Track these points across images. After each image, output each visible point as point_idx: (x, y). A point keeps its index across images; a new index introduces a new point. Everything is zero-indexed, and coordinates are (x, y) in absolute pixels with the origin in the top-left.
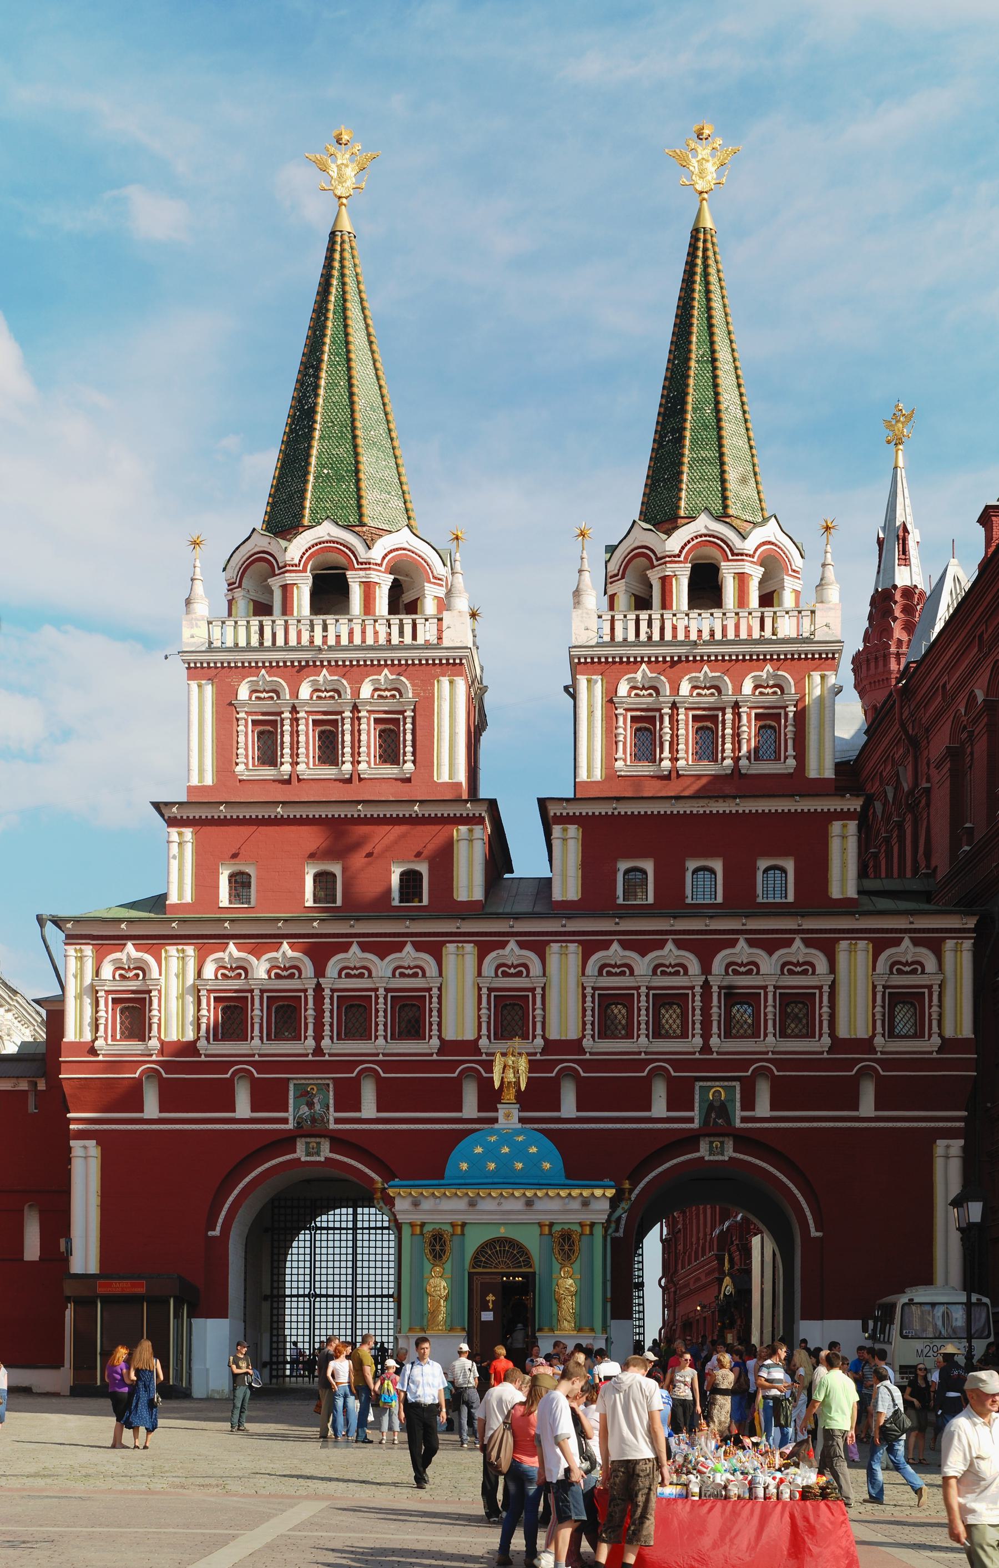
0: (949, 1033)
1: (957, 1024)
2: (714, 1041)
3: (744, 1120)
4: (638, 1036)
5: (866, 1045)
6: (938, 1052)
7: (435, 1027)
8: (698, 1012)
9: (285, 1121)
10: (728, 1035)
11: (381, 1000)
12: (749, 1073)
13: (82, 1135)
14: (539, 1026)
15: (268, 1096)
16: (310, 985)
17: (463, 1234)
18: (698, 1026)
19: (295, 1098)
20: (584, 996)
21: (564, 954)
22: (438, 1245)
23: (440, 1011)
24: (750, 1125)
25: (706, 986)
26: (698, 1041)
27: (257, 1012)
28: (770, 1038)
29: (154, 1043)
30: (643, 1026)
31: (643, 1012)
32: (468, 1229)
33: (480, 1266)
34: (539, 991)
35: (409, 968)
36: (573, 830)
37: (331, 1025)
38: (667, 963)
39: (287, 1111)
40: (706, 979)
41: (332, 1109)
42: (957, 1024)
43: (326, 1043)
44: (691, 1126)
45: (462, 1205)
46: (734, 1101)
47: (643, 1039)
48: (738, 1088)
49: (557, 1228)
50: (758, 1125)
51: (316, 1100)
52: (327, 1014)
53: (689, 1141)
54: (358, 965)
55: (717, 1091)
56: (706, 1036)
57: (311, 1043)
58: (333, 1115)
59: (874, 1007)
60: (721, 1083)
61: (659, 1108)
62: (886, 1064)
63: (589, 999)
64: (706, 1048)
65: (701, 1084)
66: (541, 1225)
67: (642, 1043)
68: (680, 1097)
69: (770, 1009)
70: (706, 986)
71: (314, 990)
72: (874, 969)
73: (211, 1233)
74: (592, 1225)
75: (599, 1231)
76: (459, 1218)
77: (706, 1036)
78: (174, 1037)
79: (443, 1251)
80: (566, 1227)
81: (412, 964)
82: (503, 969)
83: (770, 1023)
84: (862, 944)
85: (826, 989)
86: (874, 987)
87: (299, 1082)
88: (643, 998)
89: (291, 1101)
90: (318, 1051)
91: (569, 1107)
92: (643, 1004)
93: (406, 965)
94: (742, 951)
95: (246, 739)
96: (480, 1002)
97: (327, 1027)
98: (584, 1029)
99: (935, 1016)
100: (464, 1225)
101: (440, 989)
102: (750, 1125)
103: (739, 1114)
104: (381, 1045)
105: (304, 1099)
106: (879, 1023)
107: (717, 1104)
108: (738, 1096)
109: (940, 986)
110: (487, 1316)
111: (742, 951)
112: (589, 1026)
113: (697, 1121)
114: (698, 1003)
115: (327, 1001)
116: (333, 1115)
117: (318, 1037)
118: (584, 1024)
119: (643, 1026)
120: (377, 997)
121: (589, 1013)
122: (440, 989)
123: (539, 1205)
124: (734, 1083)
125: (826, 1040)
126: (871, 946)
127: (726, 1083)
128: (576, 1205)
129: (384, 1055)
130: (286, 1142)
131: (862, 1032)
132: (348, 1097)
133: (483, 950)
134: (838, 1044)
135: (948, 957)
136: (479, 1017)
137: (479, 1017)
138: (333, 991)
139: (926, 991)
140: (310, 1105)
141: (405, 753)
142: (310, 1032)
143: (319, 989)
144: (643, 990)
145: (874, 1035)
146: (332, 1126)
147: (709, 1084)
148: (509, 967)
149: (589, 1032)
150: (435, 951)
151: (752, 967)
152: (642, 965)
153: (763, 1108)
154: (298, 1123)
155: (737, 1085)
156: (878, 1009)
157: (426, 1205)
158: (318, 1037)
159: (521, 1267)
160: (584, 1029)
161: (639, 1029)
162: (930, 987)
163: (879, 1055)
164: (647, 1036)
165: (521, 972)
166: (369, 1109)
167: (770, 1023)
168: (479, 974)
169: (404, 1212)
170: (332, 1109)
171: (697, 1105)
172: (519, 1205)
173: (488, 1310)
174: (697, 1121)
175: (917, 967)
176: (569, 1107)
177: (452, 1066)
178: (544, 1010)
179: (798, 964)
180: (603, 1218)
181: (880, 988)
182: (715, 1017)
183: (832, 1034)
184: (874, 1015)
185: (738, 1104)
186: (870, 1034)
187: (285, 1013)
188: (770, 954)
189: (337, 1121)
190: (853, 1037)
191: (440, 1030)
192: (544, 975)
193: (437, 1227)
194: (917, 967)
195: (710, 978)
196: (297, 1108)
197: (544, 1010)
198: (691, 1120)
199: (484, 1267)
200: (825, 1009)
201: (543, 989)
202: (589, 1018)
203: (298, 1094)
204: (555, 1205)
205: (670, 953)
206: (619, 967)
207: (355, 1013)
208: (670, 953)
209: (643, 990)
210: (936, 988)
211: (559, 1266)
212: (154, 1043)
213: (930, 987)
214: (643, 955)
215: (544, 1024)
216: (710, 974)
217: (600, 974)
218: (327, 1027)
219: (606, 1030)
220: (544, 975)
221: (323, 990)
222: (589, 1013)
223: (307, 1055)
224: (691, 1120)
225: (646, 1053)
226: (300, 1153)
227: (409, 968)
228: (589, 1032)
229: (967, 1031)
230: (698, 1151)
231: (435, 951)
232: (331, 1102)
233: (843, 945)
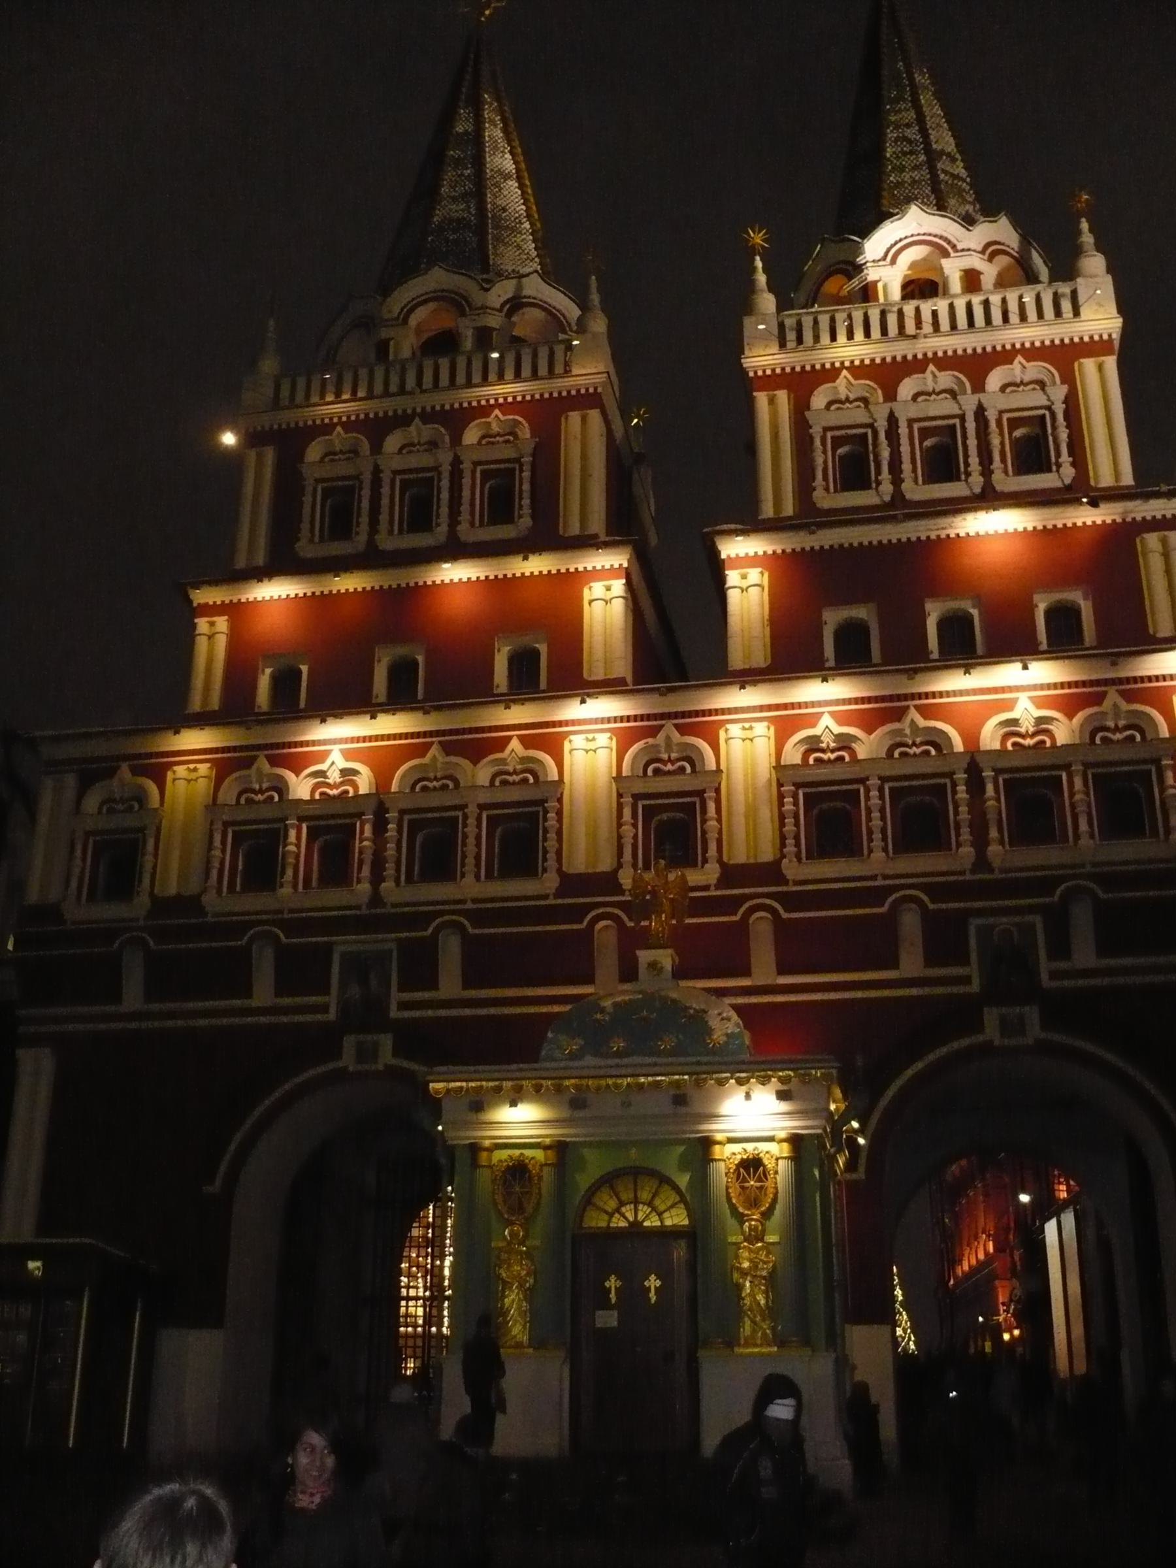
2: (994, 849)
3: (1054, 975)
4: (870, 851)
7: (551, 856)
8: (963, 809)
9: (325, 1009)
11: (471, 821)
15: (301, 971)
26: (967, 851)
29: (142, 901)
30: (877, 836)
31: (876, 815)
35: (515, 772)
39: (327, 992)
43: (387, 885)
47: (878, 855)
48: (1039, 927)
52: (391, 846)
56: (980, 842)
57: (364, 888)
58: (396, 996)
61: (911, 963)
63: (788, 800)
64: (982, 862)
67: (876, 862)
68: (944, 942)
71: (375, 814)
77: (980, 842)
78: (172, 890)
88: (874, 793)
90: (376, 899)
91: (764, 970)
92: (875, 801)
98: (783, 845)
103: (1045, 967)
104: (470, 887)
110: (608, 1319)
112: (790, 842)
114: (962, 792)
118: (783, 838)
119: (877, 836)
120: (466, 817)
129: (474, 901)
130: (325, 1042)
132: (420, 967)
136: (620, 837)
137: (620, 837)
141: (521, 507)
142: (366, 871)
144: (874, 782)
146: (394, 1013)
149: (790, 848)
153: (1085, 955)
155: (1038, 920)
160: (783, 845)
161: (870, 840)
164: (885, 850)
165: (683, 769)
166: (450, 985)
171: (974, 957)
173: (605, 1304)
176: (764, 970)
177: (578, 913)
185: (1042, 953)
189: (404, 1006)
193: (516, 1152)
196: (343, 985)
198: (967, 980)
202: (789, 827)
206: (833, 751)
209: (874, 782)
212: (142, 901)
222: (789, 821)
225: (885, 877)
226: (348, 1060)
227: (515, 772)
228: (790, 848)
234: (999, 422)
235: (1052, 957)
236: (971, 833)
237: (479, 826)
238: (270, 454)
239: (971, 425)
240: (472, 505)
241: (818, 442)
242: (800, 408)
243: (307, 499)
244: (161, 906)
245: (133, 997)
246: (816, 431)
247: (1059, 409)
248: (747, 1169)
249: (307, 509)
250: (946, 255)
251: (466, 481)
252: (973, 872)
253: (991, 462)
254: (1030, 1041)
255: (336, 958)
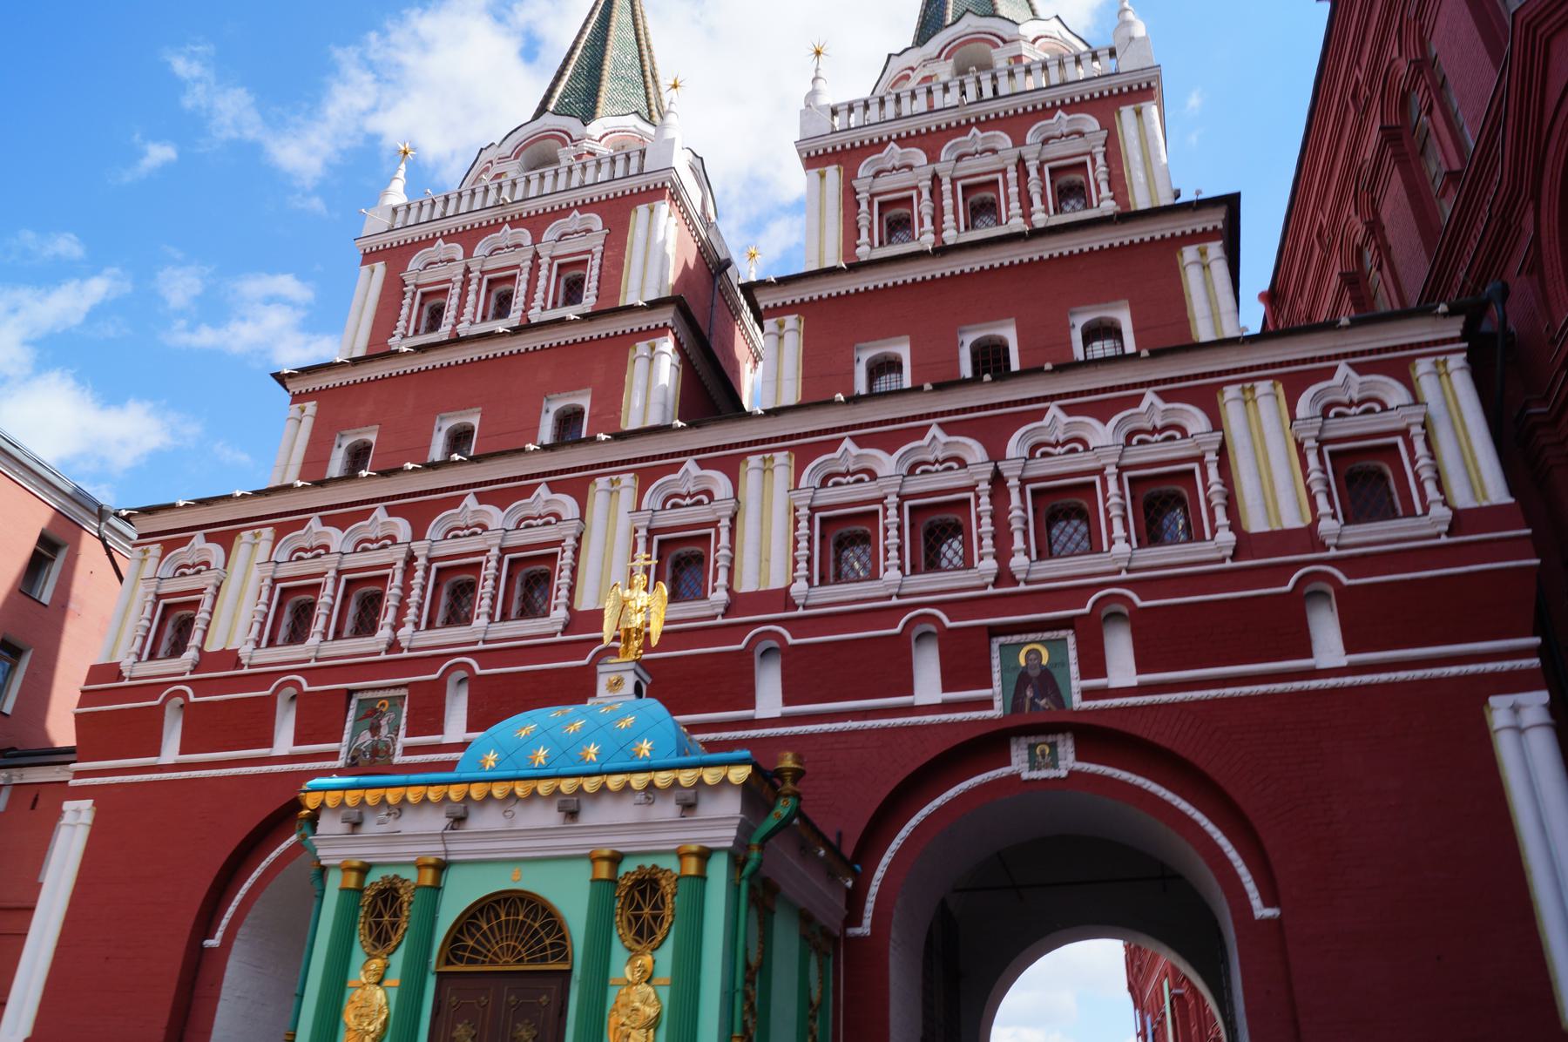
0: (1463, 499)
1: (1475, 485)
2: (1018, 562)
3: (1087, 694)
5: (1308, 538)
6: (1449, 534)
8: (986, 520)
10: (1045, 551)
12: (1087, 609)
13: (80, 793)
14: (723, 574)
16: (397, 555)
17: (437, 888)
18: (988, 542)
19: (357, 720)
20: (797, 521)
21: (766, 470)
22: (381, 909)
23: (574, 570)
24: (1101, 703)
25: (998, 480)
26: (989, 565)
27: (328, 600)
28: (1121, 548)
31: (893, 532)
32: (452, 879)
33: (460, 959)
34: (725, 522)
35: (540, 517)
36: (791, 321)
37: (420, 607)
38: (931, 458)
40: (996, 467)
41: (402, 732)
42: (1475, 485)
43: (406, 632)
44: (989, 714)
45: (436, 822)
46: (1065, 664)
48: (1071, 640)
49: (629, 866)
50: (1117, 702)
51: (383, 722)
52: (416, 592)
53: (989, 745)
54: (470, 522)
55: (1034, 651)
56: (1003, 552)
59: (1306, 476)
60: (1039, 636)
61: (928, 685)
62: (1349, 564)
63: (804, 524)
64: (1004, 576)
65: (1002, 639)
66: (594, 859)
68: (964, 666)
69: (1113, 500)
70: (998, 480)
72: (1293, 418)
73: (209, 943)
74: (704, 855)
75: (718, 870)
76: (433, 850)
77: (1003, 552)
79: (394, 926)
80: (648, 863)
81: (543, 512)
82: (672, 500)
83: (1117, 525)
84: (1263, 387)
85: (1211, 457)
86: (1300, 445)
87: (369, 695)
88: (892, 512)
89: (349, 725)
90: (394, 646)
91: (769, 699)
93: (535, 513)
94: (1056, 422)
95: (409, 310)
96: (635, 550)
97: (412, 611)
99: (1426, 474)
100: (441, 867)
101: (578, 540)
102: (1101, 703)
103: (1077, 684)
104: (481, 628)
105: (368, 722)
106: (1322, 501)
107: (1034, 673)
108: (1073, 655)
109: (1424, 426)
111: (1056, 422)
113: (998, 704)
115: (420, 574)
116: (403, 740)
117: (397, 625)
119: (893, 554)
121: (803, 544)
122: (578, 540)
123: (592, 816)
124: (1062, 633)
125: (1226, 537)
126: (1280, 388)
127: (1047, 635)
128: (668, 810)
131: (1292, 519)
132: (427, 715)
133: (646, 479)
134: (1246, 543)
135: (1428, 386)
138: (431, 560)
139: (1399, 440)
140: (375, 729)
143: (411, 559)
144: (892, 500)
145: (1316, 521)
146: (398, 759)
147: (1016, 638)
148: (683, 497)
150: (578, 487)
151: (1077, 443)
152: (887, 464)
153: (1122, 668)
154: (353, 758)
156: (1315, 475)
157: (371, 827)
158: (397, 625)
159: (544, 960)
162: (1405, 433)
163: (1333, 552)
164: (901, 568)
167: (1117, 525)
168: (639, 509)
169: (333, 840)
170: (402, 732)
171: (996, 676)
172: (550, 817)
174: (998, 704)
175: (1371, 404)
176: (769, 699)
178: (732, 549)
179: (1154, 431)
180: (726, 836)
181: (1310, 444)
182: (1016, 525)
183: (1235, 525)
184: (1308, 489)
185: (1074, 669)
186: (1309, 520)
187: (365, 602)
188: (1105, 422)
189: (408, 750)
190: (1277, 528)
191: (571, 598)
192: (736, 496)
194: (1371, 404)
195: (1001, 465)
196: (355, 734)
197: (732, 549)
198: (987, 704)
199: (471, 961)
200: (1216, 488)
201: (733, 520)
203: (362, 714)
204: (627, 812)
205: (937, 441)
207: (455, 591)
208: (937, 441)
210: (1416, 430)
211: (627, 955)
212: (190, 655)
213: (1405, 433)
214: (891, 452)
215: (731, 570)
216: (1004, 459)
217: (824, 484)
218: (412, 611)
219: (832, 572)
220: (736, 496)
221: (416, 559)
223: (378, 653)
224: (987, 704)
227: (540, 517)
229: (1496, 492)
230: (1009, 763)
231: (578, 487)
232: (404, 720)
233: (1231, 392)
234: (1040, 171)
235: (1083, 676)
236: (994, 546)
237: (499, 569)
238: (380, 267)
239: (1012, 175)
240: (546, 293)
241: (864, 206)
242: (849, 177)
243: (407, 301)
244: (206, 660)
245: (171, 752)
246: (863, 197)
247: (1099, 151)
248: (642, 893)
249: (405, 311)
250: (996, 46)
251: (543, 273)
252: (996, 584)
253: (1031, 204)
254: (1063, 773)
255: (354, 702)
